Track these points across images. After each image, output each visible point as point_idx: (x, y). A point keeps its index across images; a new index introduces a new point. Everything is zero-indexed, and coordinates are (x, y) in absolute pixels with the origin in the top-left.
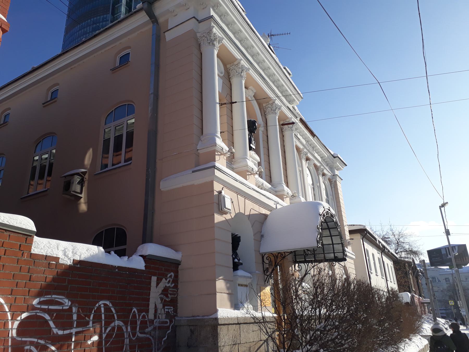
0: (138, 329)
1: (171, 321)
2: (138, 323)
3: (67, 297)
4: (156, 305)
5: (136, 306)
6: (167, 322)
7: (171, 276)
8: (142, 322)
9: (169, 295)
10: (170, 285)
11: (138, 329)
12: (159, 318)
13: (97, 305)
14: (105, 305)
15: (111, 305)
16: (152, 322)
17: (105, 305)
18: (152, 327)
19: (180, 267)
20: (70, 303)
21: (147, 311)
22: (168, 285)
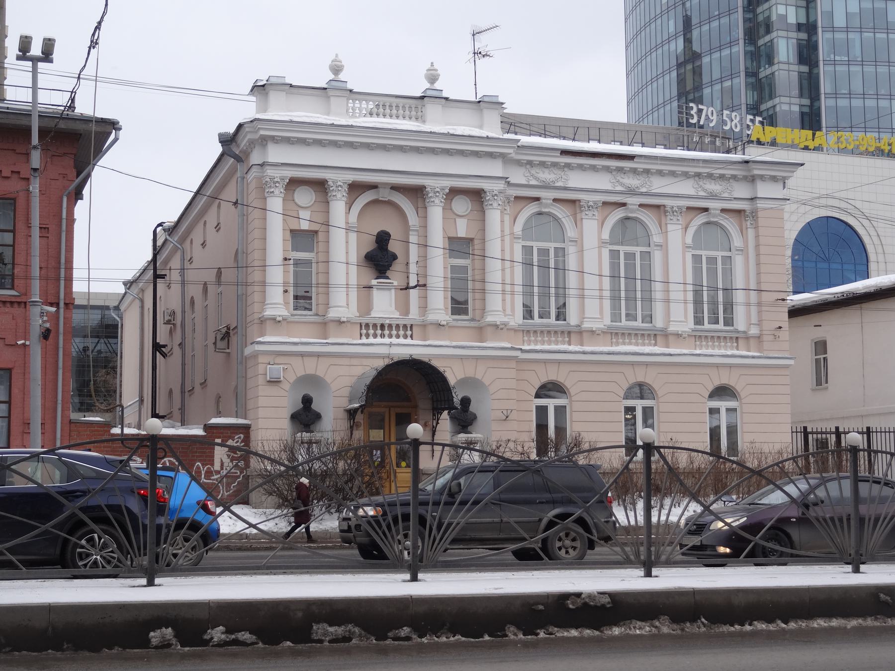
0: (203, 476)
1: (241, 473)
2: (203, 473)
3: (139, 457)
4: (221, 460)
5: (200, 461)
6: (236, 473)
7: (239, 438)
8: (206, 472)
9: (238, 452)
10: (238, 444)
11: (203, 476)
12: (226, 469)
13: (163, 461)
14: (169, 461)
15: (175, 461)
16: (218, 472)
17: (169, 461)
18: (219, 476)
19: (251, 429)
20: (141, 460)
21: (213, 465)
22: (235, 445)
